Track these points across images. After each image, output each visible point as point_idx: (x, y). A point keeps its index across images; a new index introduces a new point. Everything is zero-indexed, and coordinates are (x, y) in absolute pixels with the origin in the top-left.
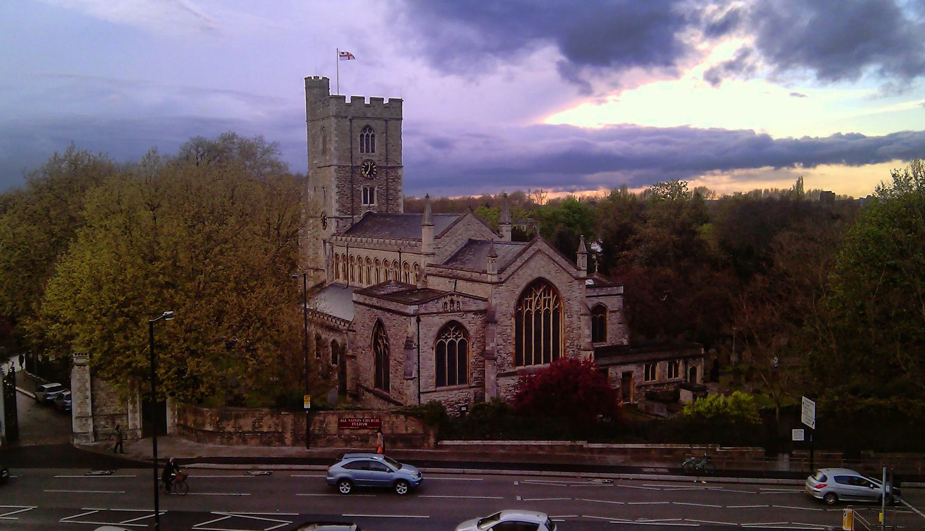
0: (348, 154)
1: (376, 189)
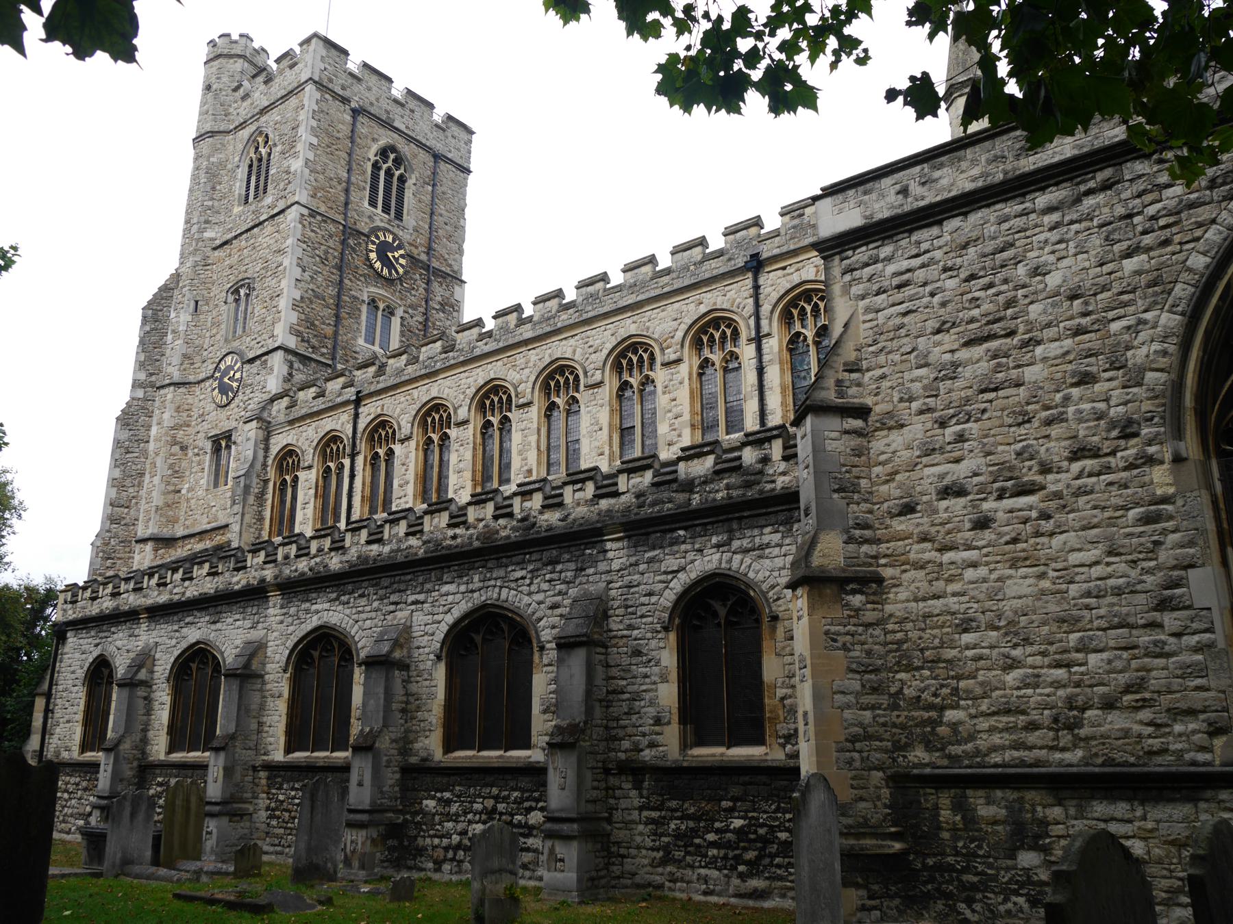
0: (337, 191)
1: (400, 312)
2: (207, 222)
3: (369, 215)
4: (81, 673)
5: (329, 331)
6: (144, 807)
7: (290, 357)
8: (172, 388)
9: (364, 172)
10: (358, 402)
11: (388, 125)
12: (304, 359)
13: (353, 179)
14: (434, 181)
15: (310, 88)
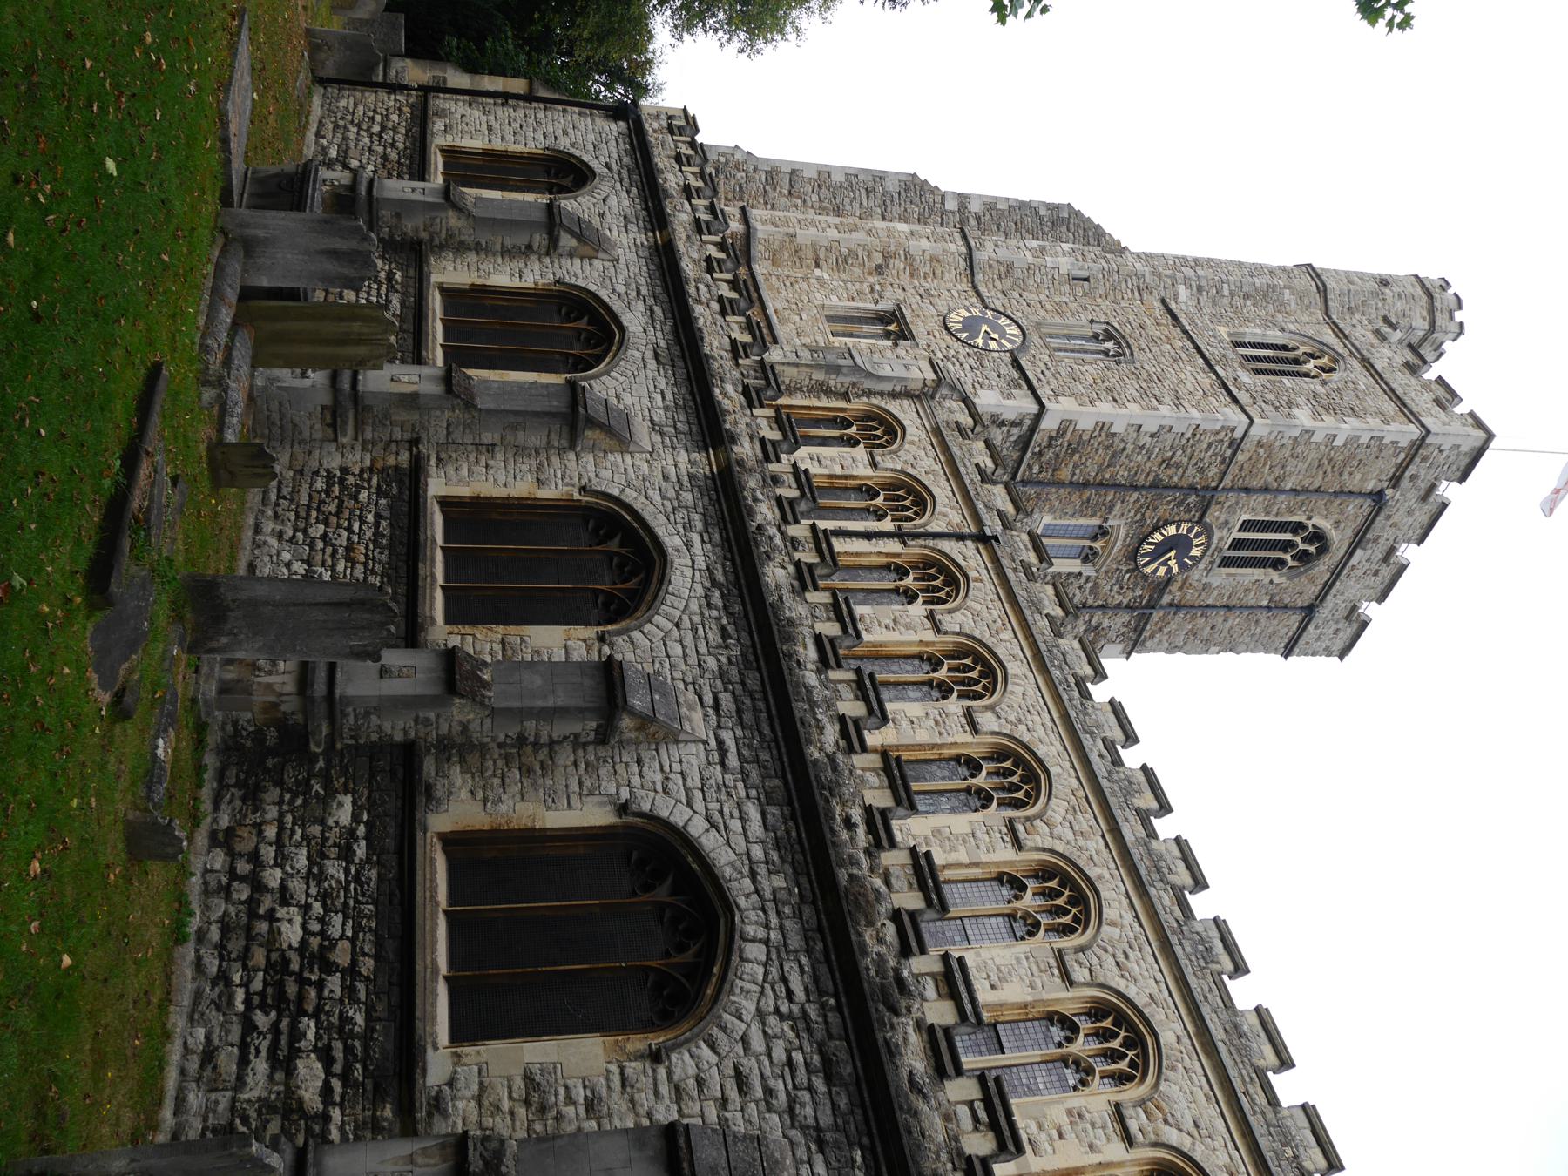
0: (1266, 476)
1: (1088, 570)
2: (1200, 289)
3: (1231, 519)
4: (564, 144)
5: (1064, 474)
6: (348, 271)
7: (1028, 422)
8: (964, 250)
9: (1291, 512)
10: (982, 538)
11: (1359, 540)
12: (1024, 443)
13: (1282, 497)
14: (1276, 607)
15: (1414, 431)
